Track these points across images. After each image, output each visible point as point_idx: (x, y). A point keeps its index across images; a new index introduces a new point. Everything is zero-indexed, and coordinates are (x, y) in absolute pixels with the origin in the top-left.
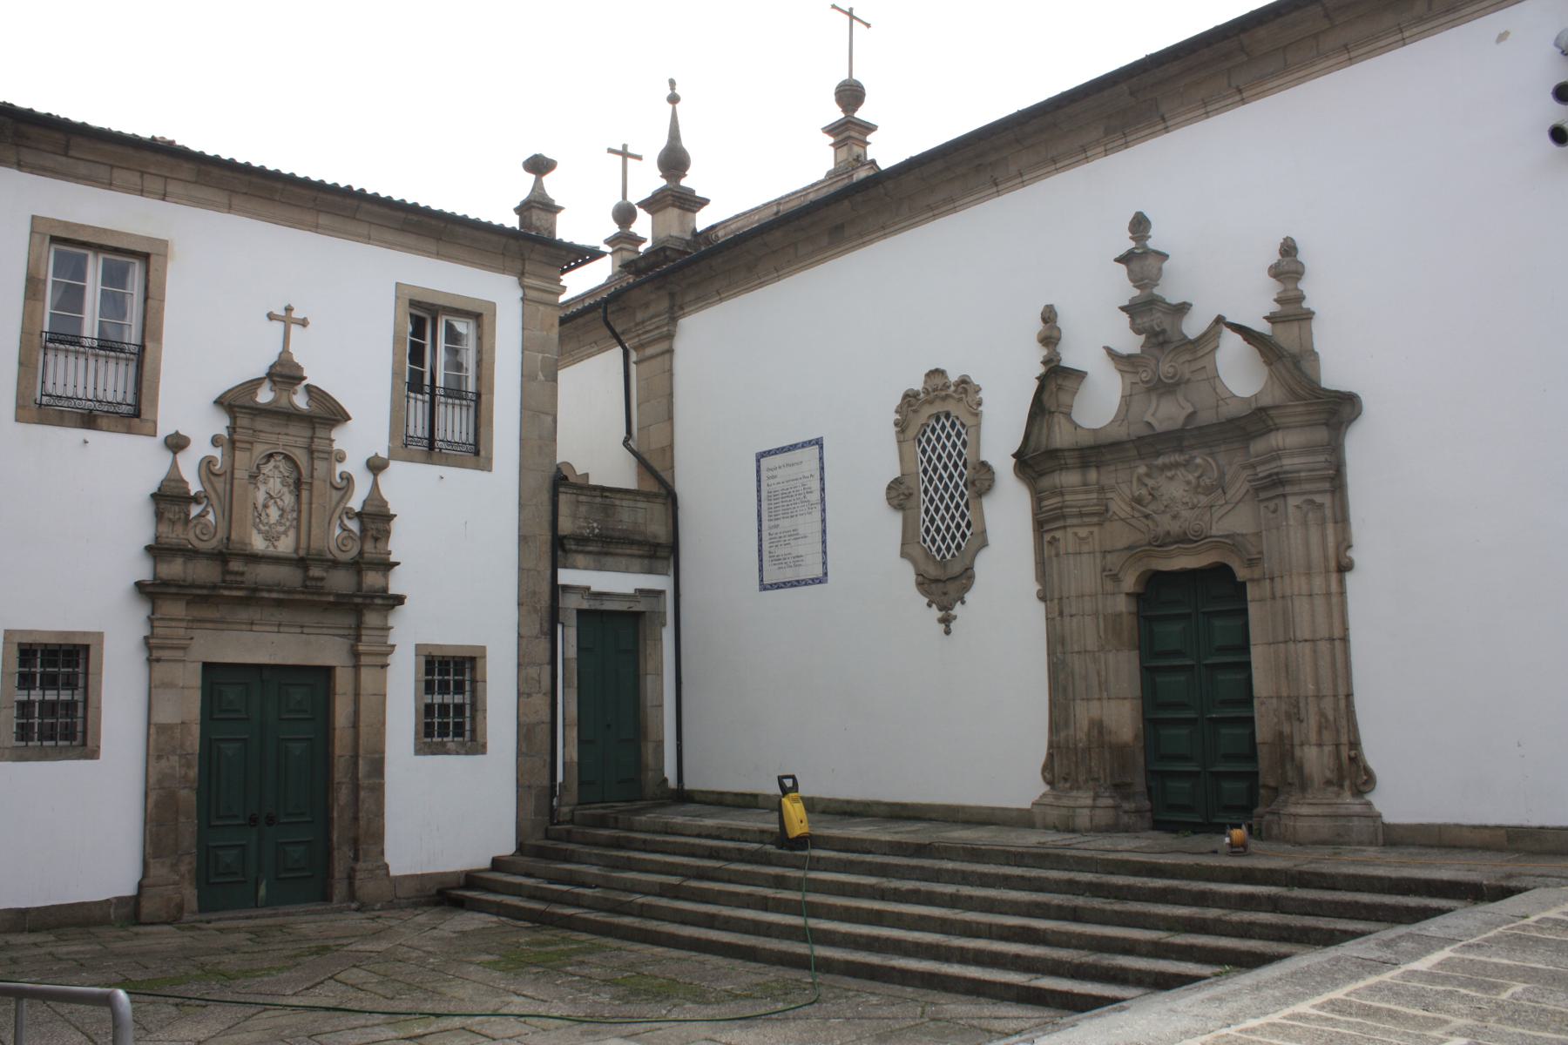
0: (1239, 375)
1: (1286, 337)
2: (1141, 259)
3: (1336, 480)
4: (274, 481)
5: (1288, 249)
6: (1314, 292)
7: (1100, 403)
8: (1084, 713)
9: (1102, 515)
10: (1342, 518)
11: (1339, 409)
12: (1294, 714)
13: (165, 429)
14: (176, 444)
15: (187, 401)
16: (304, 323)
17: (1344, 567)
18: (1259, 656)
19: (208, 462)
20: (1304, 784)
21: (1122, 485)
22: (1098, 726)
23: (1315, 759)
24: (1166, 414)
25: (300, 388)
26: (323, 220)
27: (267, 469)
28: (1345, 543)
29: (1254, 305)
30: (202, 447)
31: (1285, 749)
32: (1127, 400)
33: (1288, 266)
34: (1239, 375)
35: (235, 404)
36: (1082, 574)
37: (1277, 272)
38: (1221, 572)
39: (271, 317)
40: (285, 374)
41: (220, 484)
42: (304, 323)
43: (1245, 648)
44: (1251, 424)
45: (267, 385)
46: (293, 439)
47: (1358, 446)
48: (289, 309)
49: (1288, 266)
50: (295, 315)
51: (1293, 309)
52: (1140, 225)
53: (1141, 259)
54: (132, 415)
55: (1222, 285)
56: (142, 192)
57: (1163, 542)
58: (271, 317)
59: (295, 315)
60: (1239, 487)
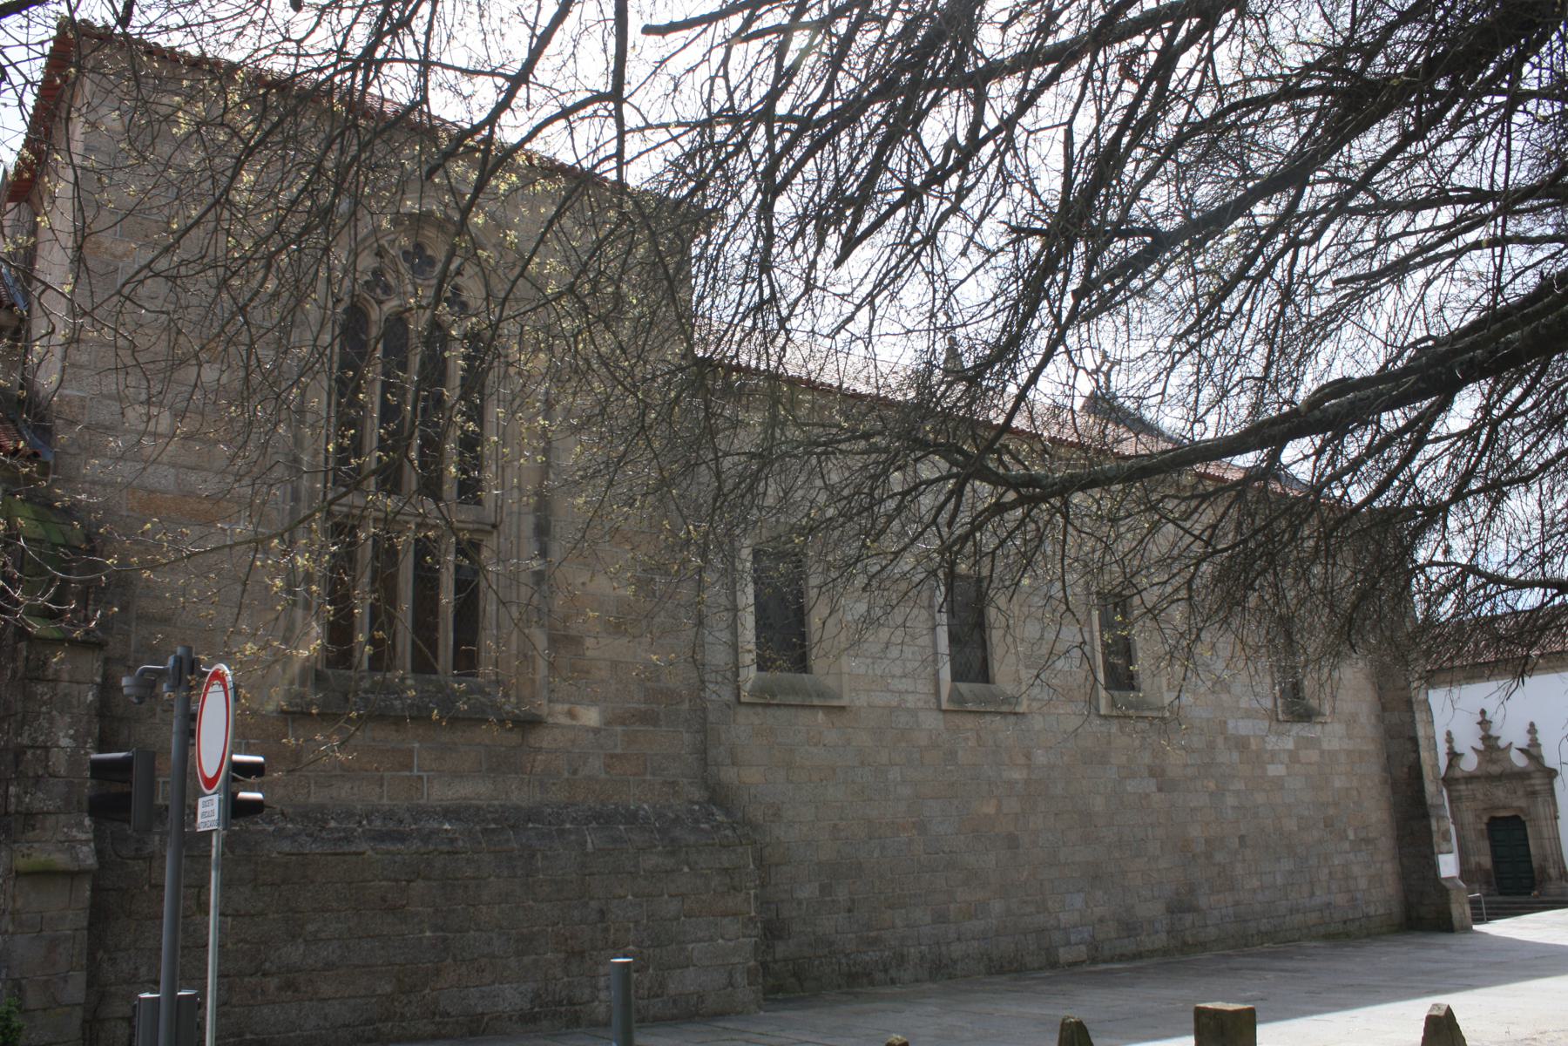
0: (1520, 761)
1: (1533, 751)
2: (1484, 723)
3: (1552, 792)
5: (1532, 725)
6: (1541, 738)
7: (1470, 763)
8: (1473, 860)
9: (1474, 799)
10: (1555, 804)
11: (1551, 774)
12: (1545, 859)
17: (1556, 818)
18: (1531, 842)
20: (1550, 879)
21: (1479, 790)
22: (1479, 864)
23: (1553, 872)
24: (1495, 769)
28: (1556, 811)
29: (1522, 740)
31: (1543, 870)
32: (1480, 764)
33: (1532, 729)
34: (1520, 761)
36: (1468, 817)
37: (1529, 732)
38: (1516, 817)
43: (1526, 839)
44: (1522, 775)
47: (1558, 784)
49: (1532, 729)
51: (1534, 743)
52: (1483, 712)
53: (1484, 723)
55: (1512, 734)
57: (1498, 808)
60: (1520, 793)
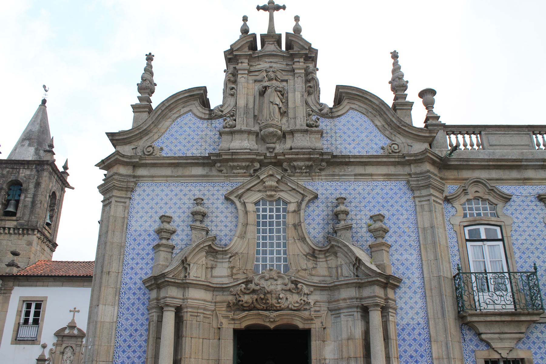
4: (69, 353)
13: (41, 344)
14: (44, 347)
15: (48, 336)
16: (78, 311)
19: (51, 350)
25: (76, 329)
26: (85, 284)
27: (67, 350)
30: (50, 346)
35: (60, 335)
39: (71, 311)
40: (72, 326)
41: (53, 355)
42: (78, 311)
45: (68, 329)
46: (72, 342)
48: (75, 308)
50: (76, 310)
54: (33, 341)
56: (43, 286)
58: (71, 311)
59: (76, 310)
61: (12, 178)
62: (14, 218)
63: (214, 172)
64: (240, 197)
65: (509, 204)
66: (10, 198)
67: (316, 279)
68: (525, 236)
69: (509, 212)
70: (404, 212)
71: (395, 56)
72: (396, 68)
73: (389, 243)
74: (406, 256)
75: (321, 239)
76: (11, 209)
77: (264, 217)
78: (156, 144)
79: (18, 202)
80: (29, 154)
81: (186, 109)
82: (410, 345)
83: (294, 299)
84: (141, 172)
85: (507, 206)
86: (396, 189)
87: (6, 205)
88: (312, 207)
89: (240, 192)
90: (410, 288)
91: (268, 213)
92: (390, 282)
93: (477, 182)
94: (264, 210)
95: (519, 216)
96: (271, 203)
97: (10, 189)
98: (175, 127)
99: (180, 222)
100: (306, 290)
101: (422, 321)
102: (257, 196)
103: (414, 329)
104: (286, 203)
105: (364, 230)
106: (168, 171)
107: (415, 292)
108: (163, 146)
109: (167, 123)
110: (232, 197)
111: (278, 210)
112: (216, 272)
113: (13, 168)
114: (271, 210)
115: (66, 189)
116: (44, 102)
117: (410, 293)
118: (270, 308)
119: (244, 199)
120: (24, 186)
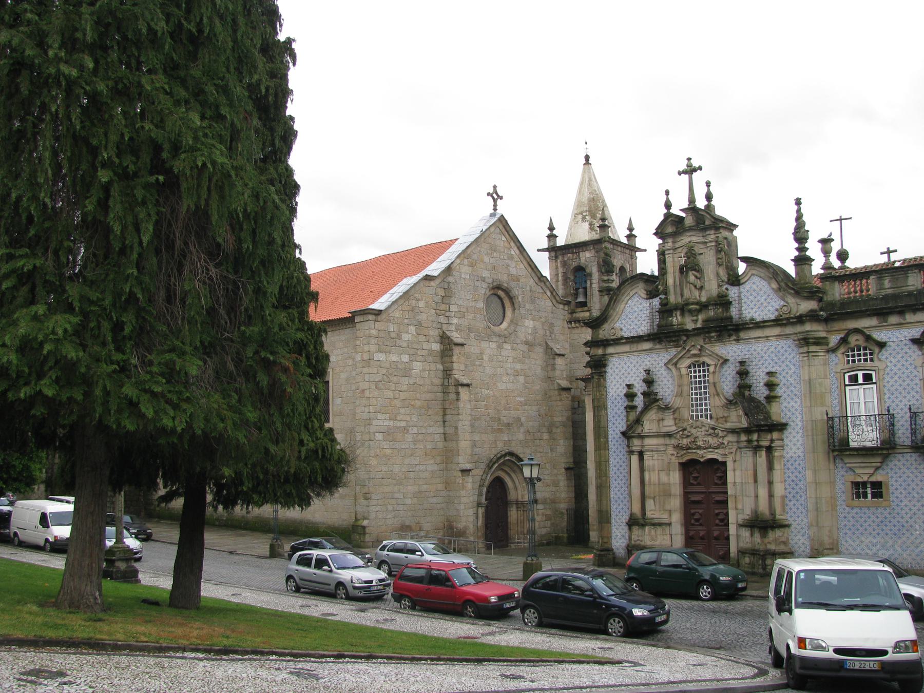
61: (575, 264)
62: (586, 309)
63: (658, 346)
64: (676, 364)
65: (883, 350)
66: (578, 286)
67: (729, 425)
68: (896, 378)
69: (884, 357)
70: (792, 367)
71: (798, 202)
72: (799, 218)
73: (779, 395)
74: (792, 403)
75: (730, 394)
76: (581, 299)
77: (695, 377)
78: (617, 325)
79: (585, 288)
80: (584, 234)
81: (634, 292)
82: (792, 473)
83: (713, 441)
84: (610, 350)
85: (883, 351)
86: (786, 347)
87: (576, 295)
88: (726, 367)
89: (675, 361)
90: (794, 429)
91: (697, 374)
92: (781, 427)
93: (857, 331)
94: (695, 372)
95: (893, 360)
96: (699, 366)
97: (575, 277)
98: (627, 310)
99: (639, 388)
100: (721, 434)
101: (801, 455)
102: (688, 362)
103: (795, 461)
104: (708, 366)
105: (762, 384)
106: (626, 348)
107: (798, 433)
108: (622, 326)
109: (622, 306)
110: (670, 366)
111: (704, 371)
112: (666, 423)
113: (573, 253)
114: (700, 371)
115: (638, 254)
116: (587, 158)
117: (794, 434)
118: (699, 448)
119: (678, 366)
120: (588, 271)
